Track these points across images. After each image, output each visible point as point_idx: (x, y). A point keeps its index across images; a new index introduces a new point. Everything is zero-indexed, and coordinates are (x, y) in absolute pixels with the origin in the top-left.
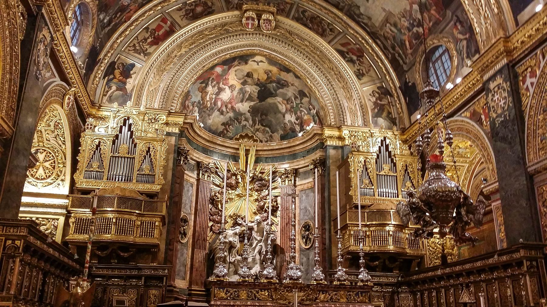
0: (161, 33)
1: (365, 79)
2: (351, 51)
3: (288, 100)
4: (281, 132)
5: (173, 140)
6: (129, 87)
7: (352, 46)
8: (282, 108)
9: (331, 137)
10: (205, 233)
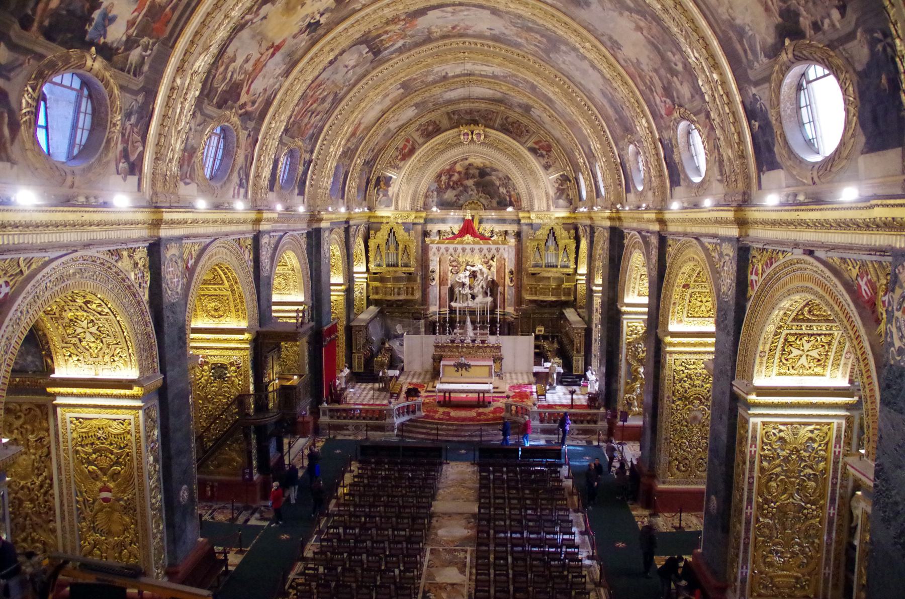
0: (406, 150)
1: (551, 170)
2: (542, 148)
3: (500, 179)
4: (497, 199)
5: (419, 227)
6: (390, 193)
7: (543, 143)
8: (497, 183)
9: (524, 218)
10: (446, 274)
